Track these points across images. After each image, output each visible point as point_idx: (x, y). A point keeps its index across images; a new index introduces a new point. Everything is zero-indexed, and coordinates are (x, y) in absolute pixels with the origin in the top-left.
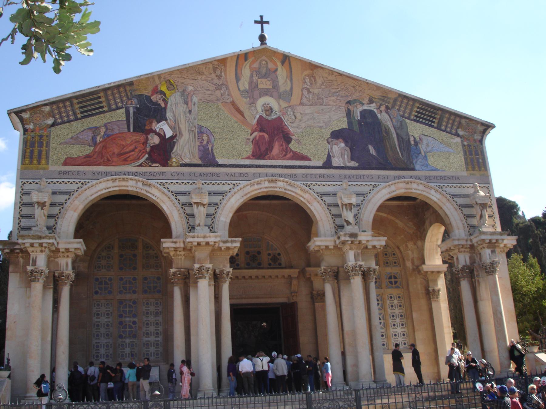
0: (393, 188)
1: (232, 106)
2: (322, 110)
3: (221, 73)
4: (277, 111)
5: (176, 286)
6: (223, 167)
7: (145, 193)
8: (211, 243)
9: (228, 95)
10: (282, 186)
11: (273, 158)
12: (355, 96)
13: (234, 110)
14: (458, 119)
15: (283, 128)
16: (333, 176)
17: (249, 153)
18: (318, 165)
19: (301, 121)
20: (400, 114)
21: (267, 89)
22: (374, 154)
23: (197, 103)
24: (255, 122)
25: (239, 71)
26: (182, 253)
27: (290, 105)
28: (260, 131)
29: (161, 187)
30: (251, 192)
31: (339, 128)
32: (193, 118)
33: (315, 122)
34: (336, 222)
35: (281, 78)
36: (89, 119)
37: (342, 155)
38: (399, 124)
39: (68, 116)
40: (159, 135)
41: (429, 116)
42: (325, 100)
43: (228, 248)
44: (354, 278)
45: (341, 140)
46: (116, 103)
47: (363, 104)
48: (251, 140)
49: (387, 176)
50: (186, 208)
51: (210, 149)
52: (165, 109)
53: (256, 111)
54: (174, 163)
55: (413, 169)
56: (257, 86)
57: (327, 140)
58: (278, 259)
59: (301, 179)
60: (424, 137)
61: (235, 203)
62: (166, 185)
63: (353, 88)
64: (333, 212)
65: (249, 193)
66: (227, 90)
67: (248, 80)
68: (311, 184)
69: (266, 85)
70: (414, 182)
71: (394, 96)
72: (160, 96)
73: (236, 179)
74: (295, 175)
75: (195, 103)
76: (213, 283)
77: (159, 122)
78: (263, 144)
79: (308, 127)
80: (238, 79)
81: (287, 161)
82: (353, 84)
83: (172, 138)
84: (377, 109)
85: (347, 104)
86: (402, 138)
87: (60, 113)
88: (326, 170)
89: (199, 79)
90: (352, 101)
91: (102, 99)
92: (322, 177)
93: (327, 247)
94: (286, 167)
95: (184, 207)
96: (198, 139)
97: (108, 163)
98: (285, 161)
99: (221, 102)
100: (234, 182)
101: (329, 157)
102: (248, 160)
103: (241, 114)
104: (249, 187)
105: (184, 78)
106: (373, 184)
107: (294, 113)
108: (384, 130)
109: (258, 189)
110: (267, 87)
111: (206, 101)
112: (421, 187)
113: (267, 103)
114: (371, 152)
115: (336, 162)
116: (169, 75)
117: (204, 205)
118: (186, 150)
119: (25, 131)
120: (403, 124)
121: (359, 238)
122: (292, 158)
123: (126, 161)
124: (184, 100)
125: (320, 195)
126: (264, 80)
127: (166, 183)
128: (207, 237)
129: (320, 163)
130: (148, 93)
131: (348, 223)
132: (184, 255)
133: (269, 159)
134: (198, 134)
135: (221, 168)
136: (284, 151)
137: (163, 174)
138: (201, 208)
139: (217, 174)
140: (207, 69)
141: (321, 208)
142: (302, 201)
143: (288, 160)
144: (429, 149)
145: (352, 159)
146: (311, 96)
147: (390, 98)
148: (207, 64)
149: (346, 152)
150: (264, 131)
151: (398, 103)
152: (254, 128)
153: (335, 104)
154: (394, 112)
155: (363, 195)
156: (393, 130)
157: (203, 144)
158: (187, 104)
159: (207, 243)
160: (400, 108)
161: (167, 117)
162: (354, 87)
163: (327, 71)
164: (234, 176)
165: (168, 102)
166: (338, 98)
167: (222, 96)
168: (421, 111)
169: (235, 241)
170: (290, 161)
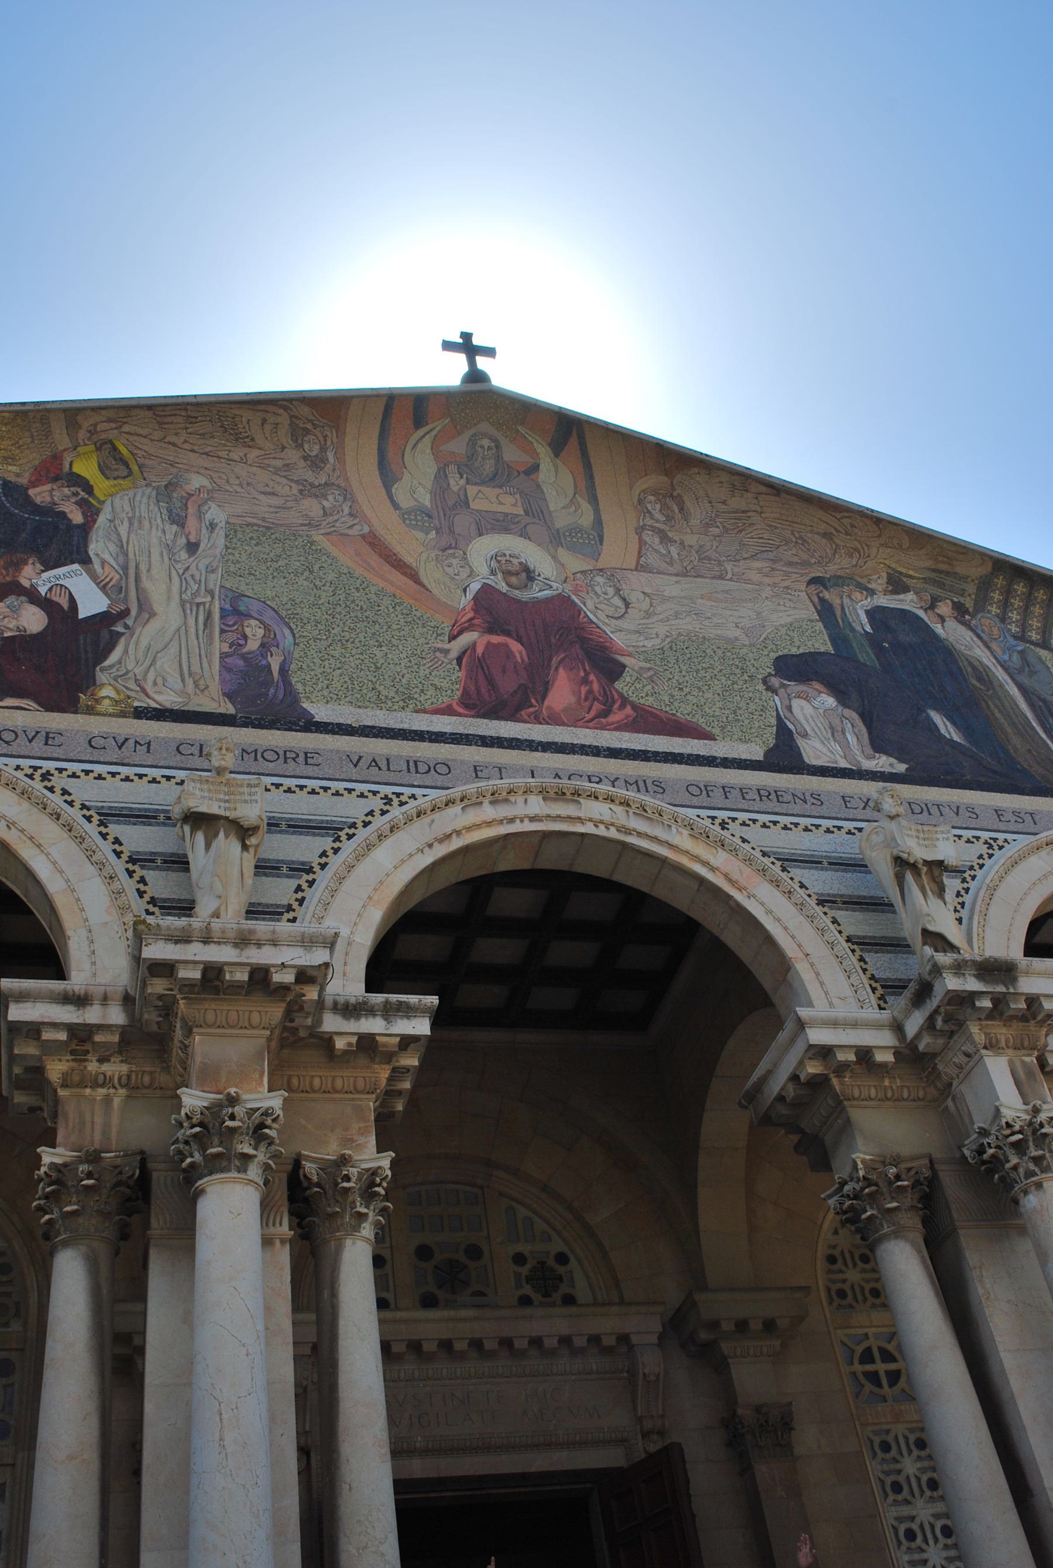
1: (366, 549)
2: (727, 592)
3: (323, 449)
4: (553, 579)
5: (65, 1244)
6: (334, 733)
8: (277, 978)
9: (351, 515)
10: (607, 816)
11: (554, 720)
12: (836, 567)
13: (375, 560)
16: (816, 796)
17: (452, 694)
18: (744, 756)
19: (648, 614)
20: (1009, 630)
21: (506, 515)
22: (956, 737)
23: (223, 524)
24: (465, 601)
26: (115, 1068)
27: (600, 566)
28: (490, 631)
30: (469, 829)
31: (801, 651)
32: (202, 566)
33: (706, 623)
34: (871, 970)
35: (554, 493)
37: (835, 732)
38: (1015, 657)
42: (729, 566)
43: (367, 1043)
44: (1039, 1186)
45: (816, 685)
48: (454, 654)
49: (1031, 814)
50: (150, 875)
51: (275, 668)
52: (85, 529)
53: (467, 570)
54: (107, 702)
56: (467, 504)
57: (765, 681)
58: (560, 1279)
59: (686, 799)
61: (395, 867)
62: (59, 782)
63: (824, 540)
64: (850, 930)
65: (458, 833)
66: (349, 503)
67: (429, 482)
68: (734, 819)
69: (500, 503)
71: (977, 571)
72: (66, 491)
73: (392, 777)
74: (659, 787)
75: (212, 526)
76: (284, 1228)
77: (48, 566)
78: (504, 672)
79: (680, 634)
80: (388, 476)
81: (617, 734)
82: (822, 528)
84: (926, 610)
85: (813, 587)
86: (1044, 701)
88: (785, 775)
89: (237, 458)
90: (829, 579)
92: (773, 796)
93: (864, 1054)
94: (614, 753)
95: (139, 872)
96: (222, 631)
98: (606, 734)
99: (322, 531)
100: (388, 790)
102: (446, 719)
103: (405, 574)
104: (456, 809)
105: (174, 445)
106: (985, 835)
107: (620, 590)
108: (969, 669)
109: (501, 822)
111: (260, 522)
113: (507, 553)
114: (943, 731)
116: (110, 420)
117: (243, 832)
118: (167, 663)
120: (1031, 659)
121: (1028, 985)
124: (170, 511)
125: (778, 863)
126: (491, 492)
127: (61, 770)
128: (259, 945)
129: (755, 752)
130: (18, 475)
132: (126, 1083)
133: (538, 719)
134: (222, 617)
135: (328, 737)
136: (595, 699)
138: (227, 845)
140: (267, 427)
141: (793, 910)
142: (702, 881)
143: (617, 729)
145: (878, 746)
146: (674, 550)
147: (964, 578)
148: (271, 408)
149: (849, 725)
150: (507, 633)
151: (996, 596)
152: (464, 620)
153: (767, 580)
154: (988, 620)
156: (1000, 674)
157: (245, 650)
158: (182, 525)
159: (260, 976)
160: (1004, 613)
161: (91, 553)
162: (826, 535)
163: (725, 477)
164: (383, 765)
165: (98, 512)
166: (776, 566)
167: (325, 514)
169: (407, 1011)
170: (627, 735)
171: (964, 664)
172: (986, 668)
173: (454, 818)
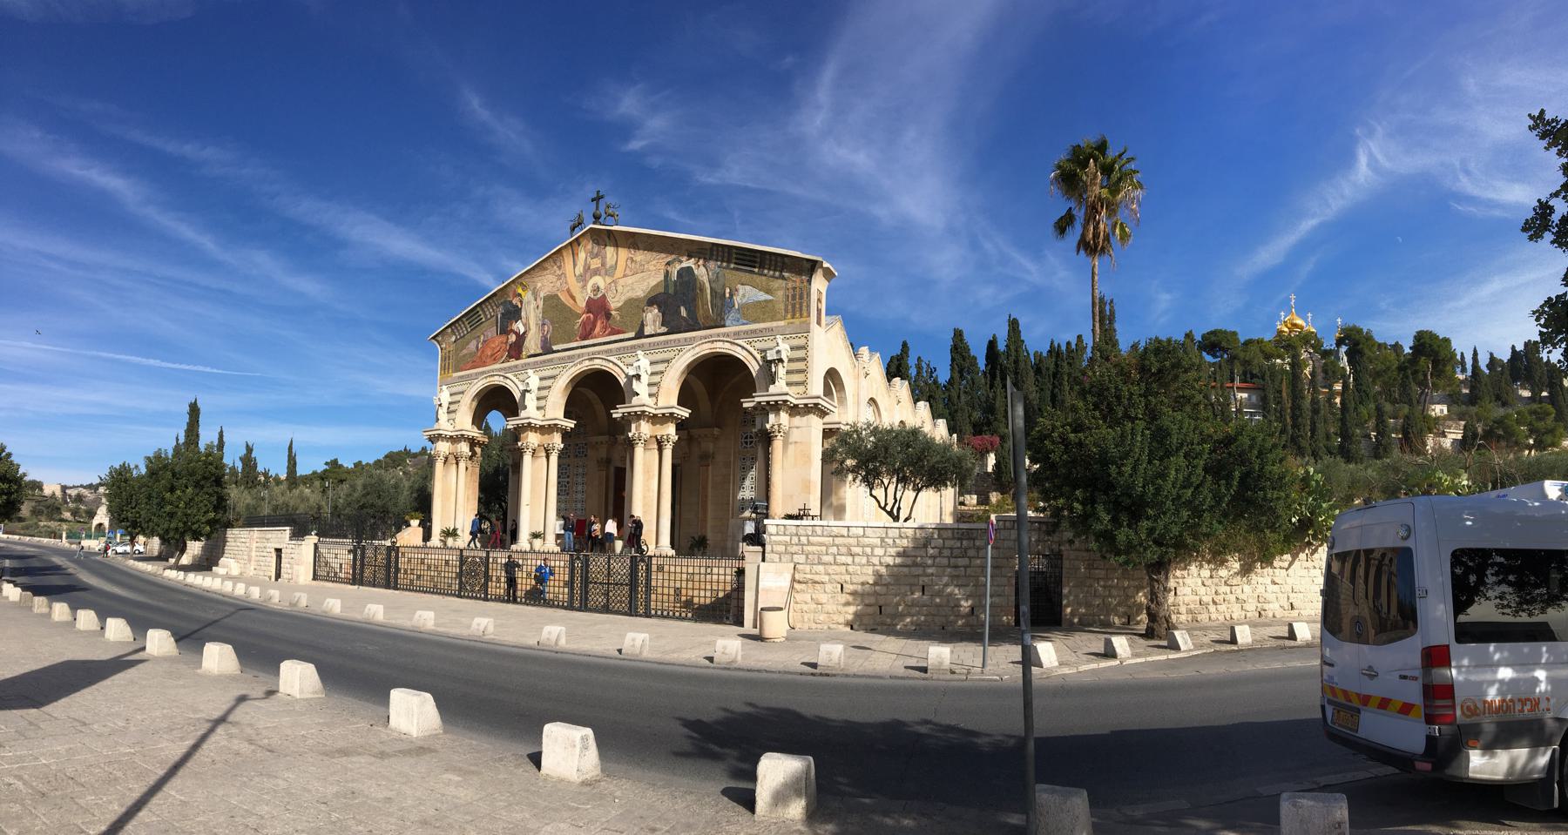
0: (697, 349)
7: (504, 384)
13: (568, 297)
14: (779, 259)
15: (605, 305)
24: (584, 304)
25: (576, 257)
28: (588, 313)
29: (514, 379)
36: (474, 331)
39: (463, 332)
40: (516, 333)
41: (750, 261)
42: (646, 266)
46: (490, 313)
47: (681, 262)
55: (724, 326)
60: (739, 286)
70: (719, 341)
71: (708, 247)
74: (611, 350)
83: (524, 333)
87: (458, 331)
91: (481, 312)
94: (605, 344)
97: (484, 364)
101: (642, 326)
106: (679, 348)
110: (597, 266)
112: (727, 345)
115: (648, 331)
118: (532, 343)
119: (442, 349)
120: (720, 275)
122: (609, 334)
123: (495, 361)
126: (594, 260)
129: (632, 335)
131: (638, 394)
133: (592, 338)
137: (516, 366)
139: (551, 360)
144: (744, 301)
145: (663, 325)
155: (668, 361)
156: (707, 285)
168: (741, 257)
171: (698, 285)
172: (704, 283)
173: (573, 369)
